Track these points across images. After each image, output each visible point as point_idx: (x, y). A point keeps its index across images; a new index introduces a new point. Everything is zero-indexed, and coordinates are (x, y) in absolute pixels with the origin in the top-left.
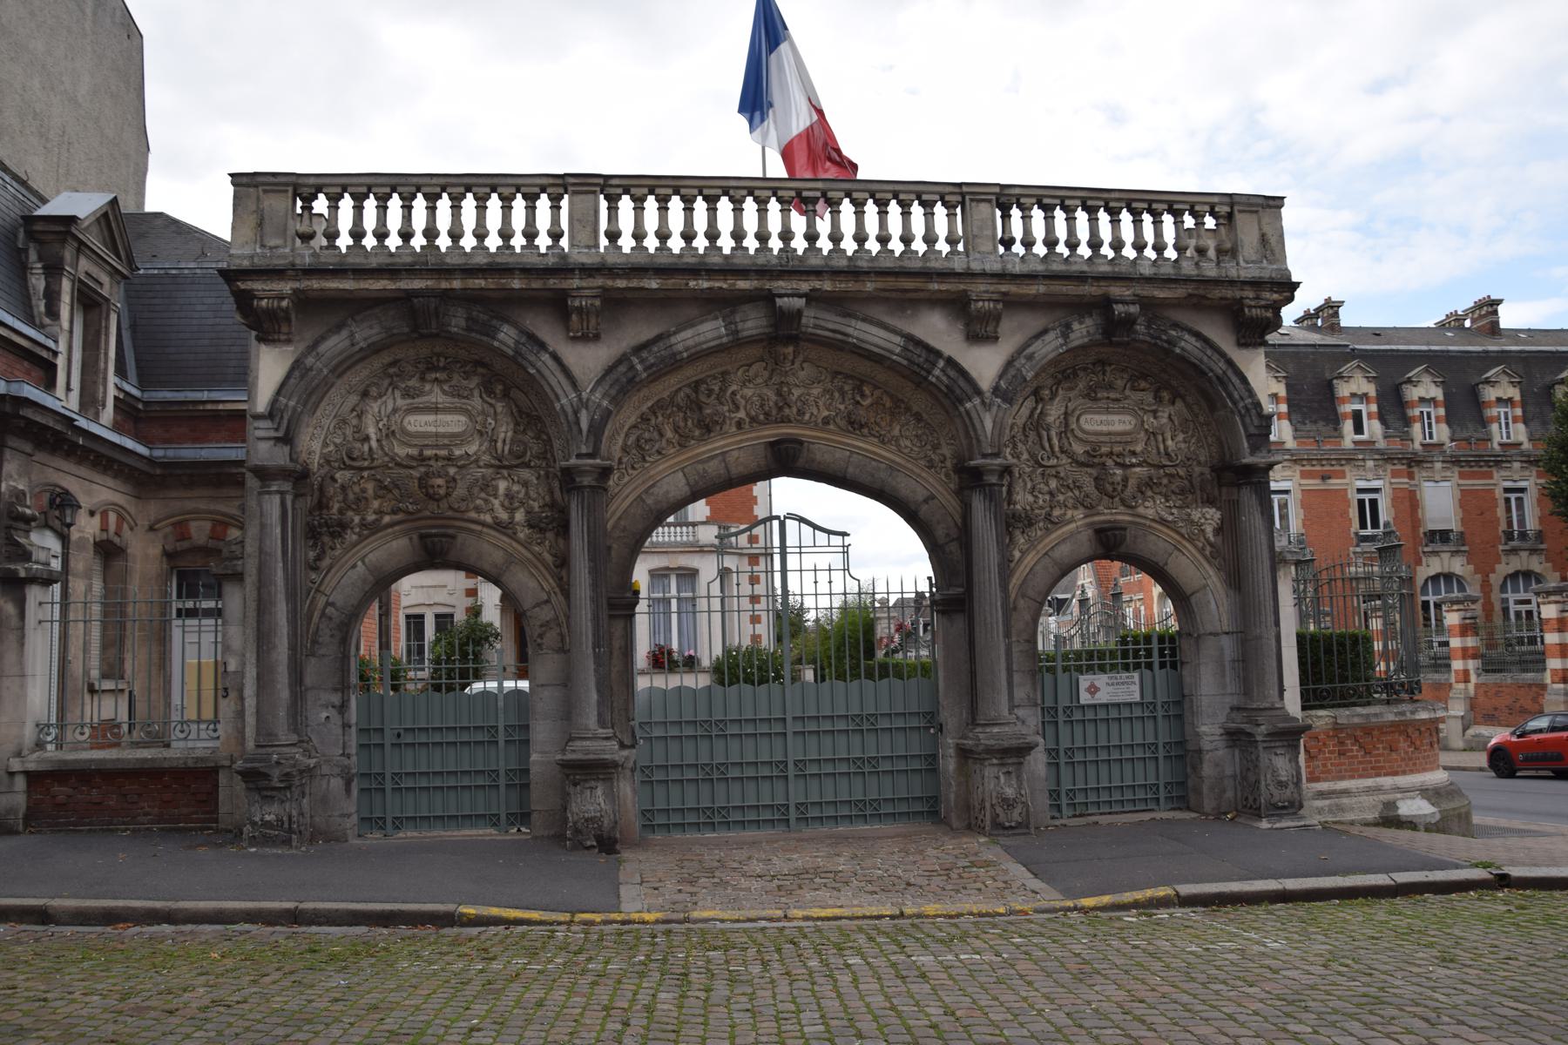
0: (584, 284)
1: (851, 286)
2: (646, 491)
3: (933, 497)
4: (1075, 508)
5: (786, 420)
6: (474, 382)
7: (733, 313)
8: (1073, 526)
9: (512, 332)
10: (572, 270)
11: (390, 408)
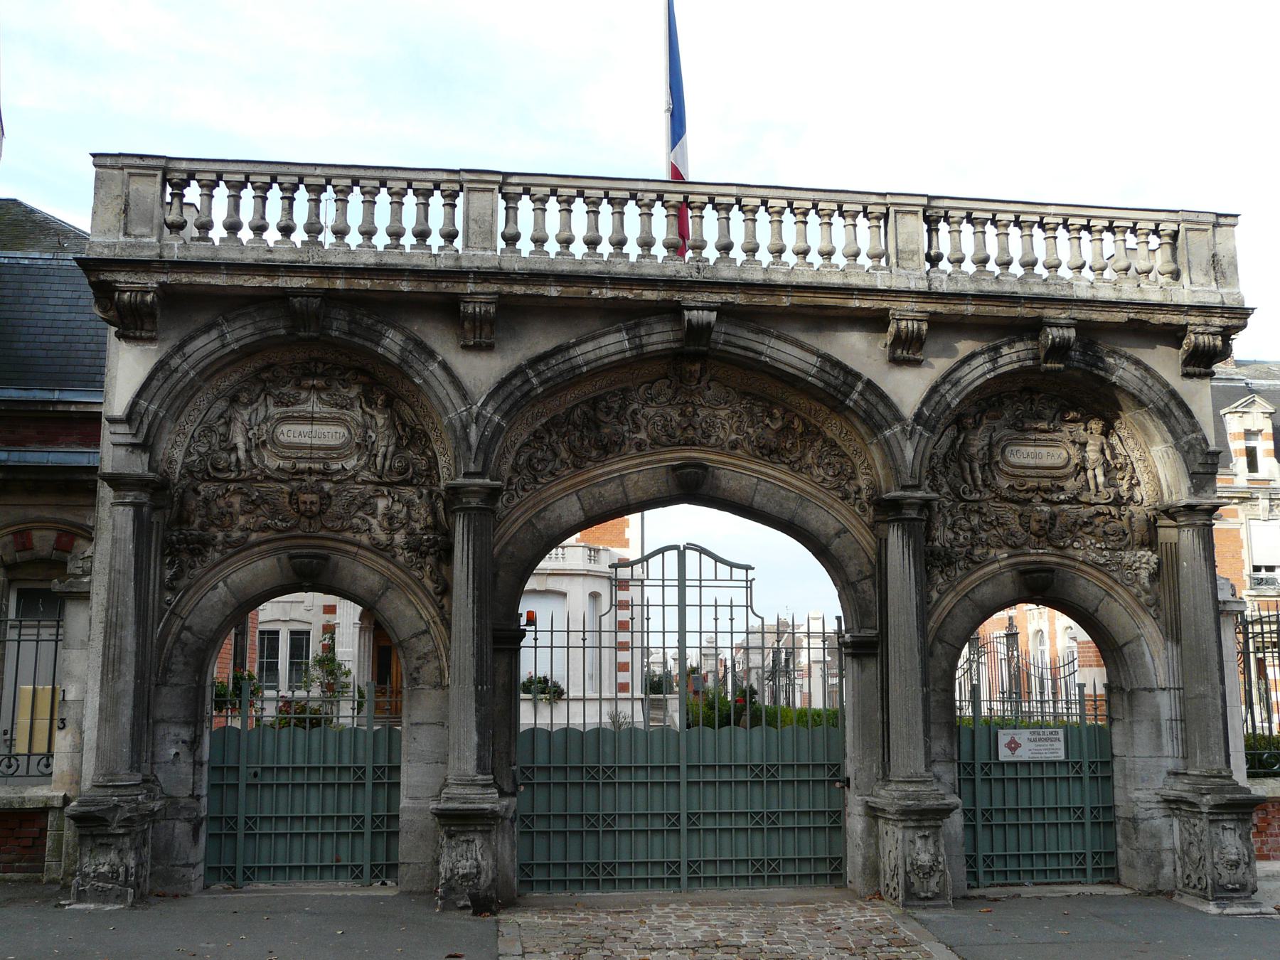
0: (479, 288)
1: (766, 300)
2: (537, 515)
3: (845, 531)
4: (1000, 547)
5: (690, 443)
6: (353, 392)
7: (637, 326)
8: (996, 566)
9: (399, 338)
10: (467, 273)
11: (262, 414)
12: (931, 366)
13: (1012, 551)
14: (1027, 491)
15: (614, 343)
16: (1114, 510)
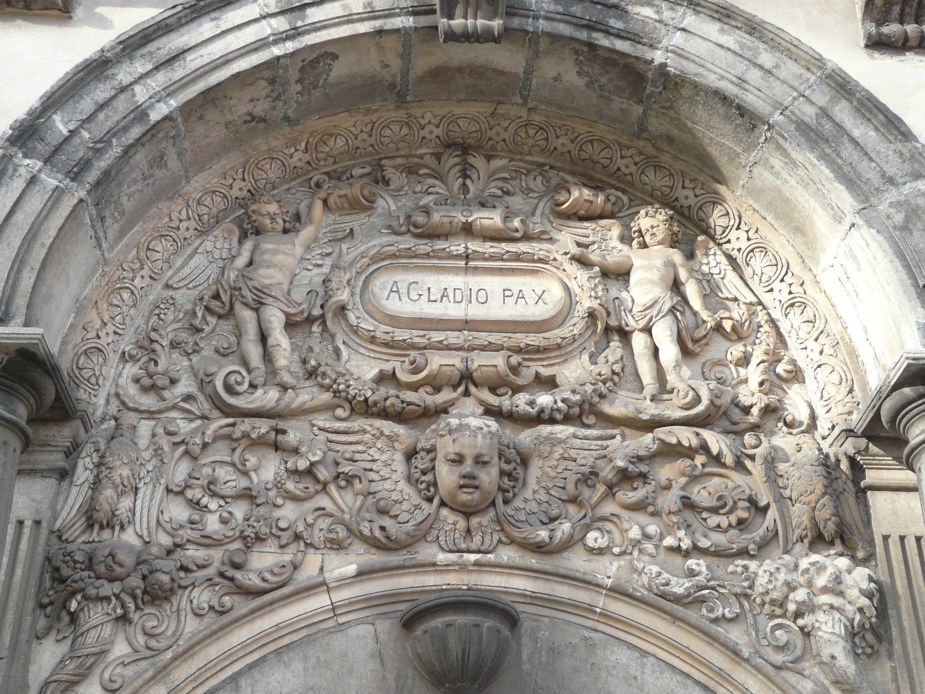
4: (337, 545)
8: (320, 601)
12: (103, 23)
13: (376, 558)
14: (435, 384)
16: (715, 440)
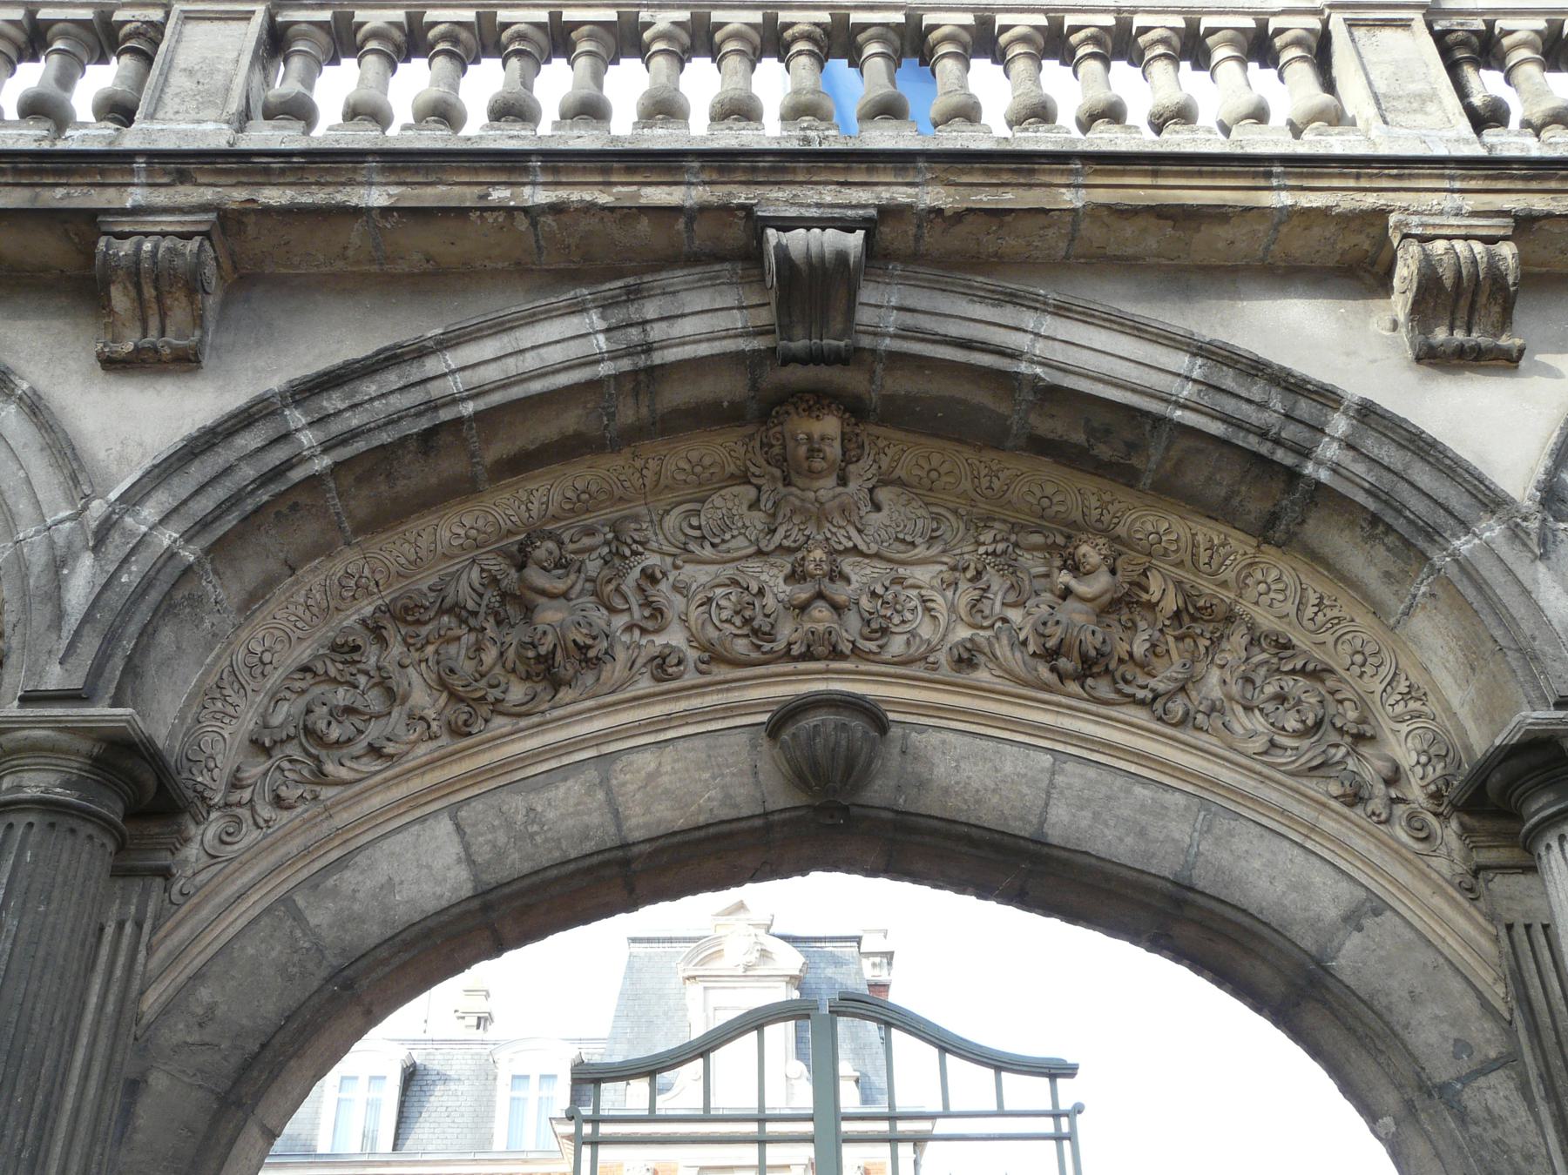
0: (161, 197)
2: (313, 883)
3: (1379, 907)
7: (634, 294)
15: (559, 343)
